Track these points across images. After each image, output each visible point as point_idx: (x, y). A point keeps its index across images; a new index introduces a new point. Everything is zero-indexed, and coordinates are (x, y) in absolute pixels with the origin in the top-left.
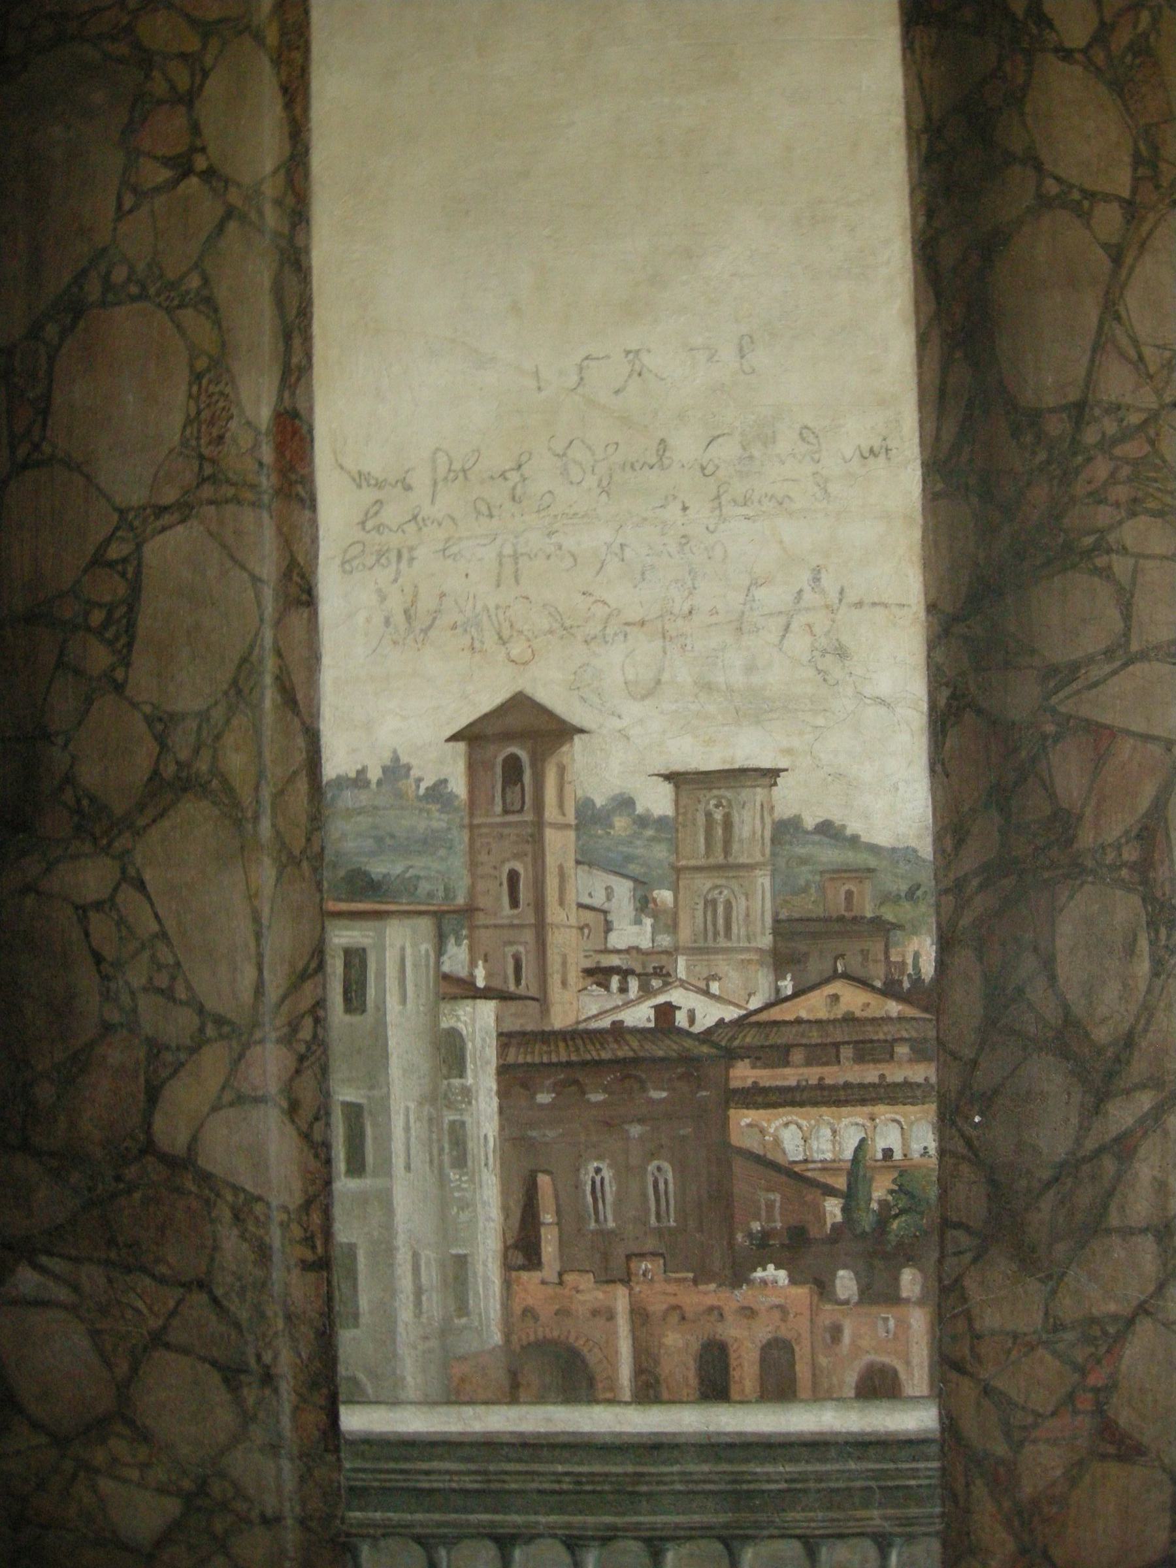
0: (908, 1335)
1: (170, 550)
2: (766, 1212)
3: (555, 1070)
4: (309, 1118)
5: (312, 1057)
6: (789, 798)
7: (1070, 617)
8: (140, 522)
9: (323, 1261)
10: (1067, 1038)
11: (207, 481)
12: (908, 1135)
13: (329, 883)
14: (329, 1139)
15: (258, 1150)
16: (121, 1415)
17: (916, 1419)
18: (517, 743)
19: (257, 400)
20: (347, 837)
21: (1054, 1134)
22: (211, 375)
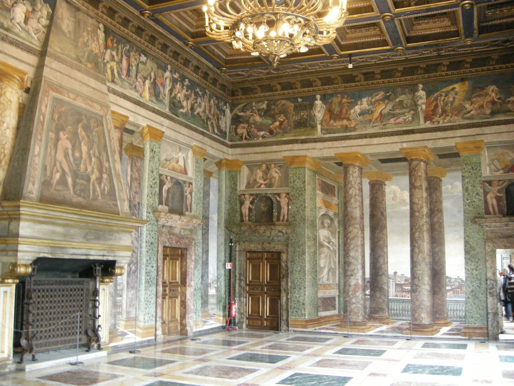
0: (409, 295)
1: (383, 266)
2: (404, 290)
3: (397, 285)
4: (388, 286)
5: (388, 284)
6: (406, 275)
7: (415, 269)
8: (382, 265)
9: (388, 292)
10: (415, 284)
11: (384, 263)
12: (409, 288)
13: (388, 278)
14: (388, 287)
15: (386, 288)
16: (380, 298)
17: (410, 298)
18: (395, 273)
19: (386, 260)
20: (389, 276)
21: (415, 288)
22: (384, 259)
